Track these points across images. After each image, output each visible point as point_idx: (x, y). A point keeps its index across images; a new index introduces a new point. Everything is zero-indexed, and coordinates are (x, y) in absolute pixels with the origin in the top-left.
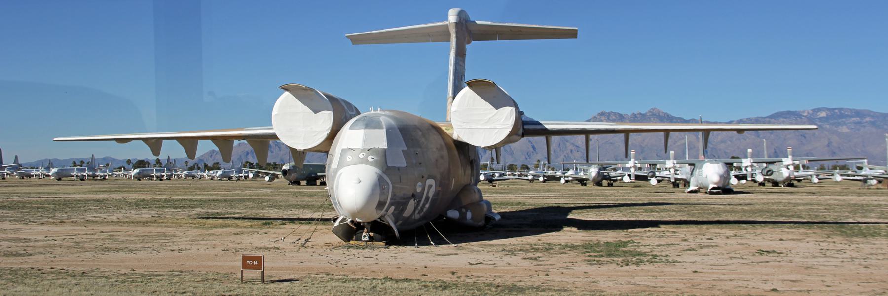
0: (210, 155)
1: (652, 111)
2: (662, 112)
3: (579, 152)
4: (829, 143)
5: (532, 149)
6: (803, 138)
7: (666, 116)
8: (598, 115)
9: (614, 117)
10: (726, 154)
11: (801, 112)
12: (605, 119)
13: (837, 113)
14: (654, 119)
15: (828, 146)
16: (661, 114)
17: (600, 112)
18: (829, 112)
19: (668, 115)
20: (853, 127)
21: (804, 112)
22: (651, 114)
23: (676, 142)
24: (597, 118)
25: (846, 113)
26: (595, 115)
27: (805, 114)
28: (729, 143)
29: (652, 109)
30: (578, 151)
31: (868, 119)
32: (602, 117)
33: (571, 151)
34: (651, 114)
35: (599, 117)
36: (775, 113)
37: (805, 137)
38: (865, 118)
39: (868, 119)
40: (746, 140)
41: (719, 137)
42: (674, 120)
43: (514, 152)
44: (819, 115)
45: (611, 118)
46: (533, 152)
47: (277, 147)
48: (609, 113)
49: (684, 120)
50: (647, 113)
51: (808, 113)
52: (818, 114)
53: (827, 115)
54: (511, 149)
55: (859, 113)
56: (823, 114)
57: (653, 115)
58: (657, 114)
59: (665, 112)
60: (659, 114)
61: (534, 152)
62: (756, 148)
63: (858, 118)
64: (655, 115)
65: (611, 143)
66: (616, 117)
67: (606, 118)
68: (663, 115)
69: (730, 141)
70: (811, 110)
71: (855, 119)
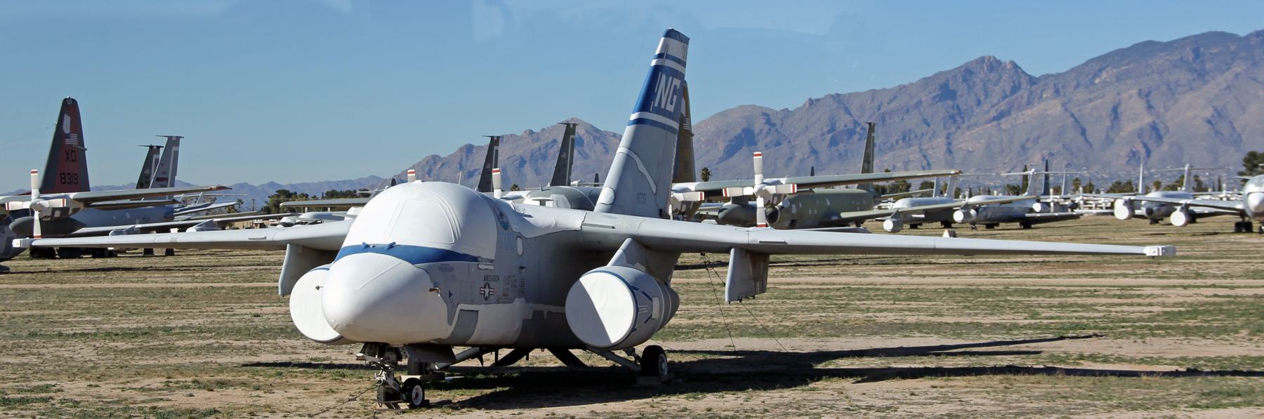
0: (427, 169)
43: (1244, 137)
47: (598, 144)
54: (1233, 128)
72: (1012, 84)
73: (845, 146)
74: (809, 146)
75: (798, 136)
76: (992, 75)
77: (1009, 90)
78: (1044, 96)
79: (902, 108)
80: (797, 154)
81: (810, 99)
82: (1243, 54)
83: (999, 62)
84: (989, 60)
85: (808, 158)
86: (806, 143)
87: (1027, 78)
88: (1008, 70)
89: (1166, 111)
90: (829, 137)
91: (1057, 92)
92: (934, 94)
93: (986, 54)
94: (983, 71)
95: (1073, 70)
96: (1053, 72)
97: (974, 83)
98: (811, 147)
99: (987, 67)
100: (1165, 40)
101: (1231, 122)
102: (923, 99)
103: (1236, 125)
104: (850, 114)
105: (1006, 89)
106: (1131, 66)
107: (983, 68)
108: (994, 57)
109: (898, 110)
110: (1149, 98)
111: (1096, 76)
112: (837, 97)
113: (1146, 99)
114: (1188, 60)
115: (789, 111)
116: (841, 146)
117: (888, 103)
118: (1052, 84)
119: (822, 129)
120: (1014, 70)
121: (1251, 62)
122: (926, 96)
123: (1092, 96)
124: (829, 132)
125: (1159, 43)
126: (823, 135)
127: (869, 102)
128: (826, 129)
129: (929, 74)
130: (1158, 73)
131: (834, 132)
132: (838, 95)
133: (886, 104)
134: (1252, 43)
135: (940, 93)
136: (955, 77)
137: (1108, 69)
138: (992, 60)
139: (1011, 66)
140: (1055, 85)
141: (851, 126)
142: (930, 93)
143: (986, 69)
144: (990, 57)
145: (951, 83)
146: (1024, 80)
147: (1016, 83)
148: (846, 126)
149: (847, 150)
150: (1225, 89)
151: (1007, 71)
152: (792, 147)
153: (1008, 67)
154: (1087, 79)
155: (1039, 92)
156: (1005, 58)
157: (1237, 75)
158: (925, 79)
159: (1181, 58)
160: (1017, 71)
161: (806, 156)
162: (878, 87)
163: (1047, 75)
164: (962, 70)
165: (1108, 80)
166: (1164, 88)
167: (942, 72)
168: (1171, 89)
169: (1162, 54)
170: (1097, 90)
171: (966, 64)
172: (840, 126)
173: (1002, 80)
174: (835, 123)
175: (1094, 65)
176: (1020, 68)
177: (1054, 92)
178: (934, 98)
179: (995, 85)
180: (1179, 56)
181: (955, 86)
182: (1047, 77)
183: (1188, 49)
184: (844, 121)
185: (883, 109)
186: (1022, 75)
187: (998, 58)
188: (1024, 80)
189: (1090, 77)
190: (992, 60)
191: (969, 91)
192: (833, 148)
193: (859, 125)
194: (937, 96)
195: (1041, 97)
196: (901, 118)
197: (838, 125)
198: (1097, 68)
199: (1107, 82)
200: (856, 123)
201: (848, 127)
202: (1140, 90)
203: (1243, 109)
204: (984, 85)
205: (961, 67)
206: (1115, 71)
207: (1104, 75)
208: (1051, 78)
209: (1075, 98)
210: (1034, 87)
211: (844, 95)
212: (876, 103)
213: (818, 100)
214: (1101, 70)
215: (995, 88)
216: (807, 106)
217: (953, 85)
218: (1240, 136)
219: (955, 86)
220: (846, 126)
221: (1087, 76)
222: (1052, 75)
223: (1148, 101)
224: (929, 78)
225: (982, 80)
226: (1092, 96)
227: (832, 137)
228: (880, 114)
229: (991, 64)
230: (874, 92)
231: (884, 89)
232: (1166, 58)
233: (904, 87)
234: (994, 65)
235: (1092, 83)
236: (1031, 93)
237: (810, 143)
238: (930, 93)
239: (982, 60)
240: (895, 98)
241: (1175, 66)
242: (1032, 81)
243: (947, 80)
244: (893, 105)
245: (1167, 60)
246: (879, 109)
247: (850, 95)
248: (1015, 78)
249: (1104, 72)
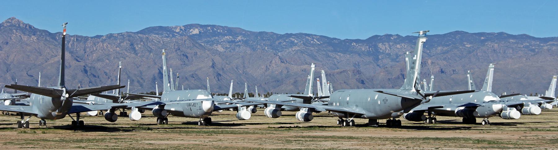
1: (10, 21)
2: (24, 24)
4: (213, 64)
6: (185, 58)
7: (28, 27)
10: (106, 75)
11: (173, 28)
13: (209, 30)
14: (17, 32)
15: (213, 66)
16: (21, 25)
18: (201, 29)
19: (30, 27)
20: (228, 46)
21: (176, 28)
22: (8, 24)
23: (48, 59)
25: (219, 31)
27: (178, 31)
28: (107, 61)
29: (10, 18)
31: (239, 38)
34: (8, 24)
36: (146, 29)
37: (187, 57)
38: (238, 37)
39: (239, 38)
40: (125, 59)
41: (94, 55)
42: (38, 33)
44: (192, 32)
49: (50, 34)
50: (3, 23)
51: (181, 30)
52: (190, 31)
53: (200, 32)
55: (230, 31)
56: (196, 31)
57: (12, 25)
58: (17, 25)
59: (26, 23)
60: (19, 25)
62: (138, 68)
63: (231, 37)
64: (15, 26)
68: (24, 26)
69: (108, 59)
70: (183, 26)
71: (228, 37)
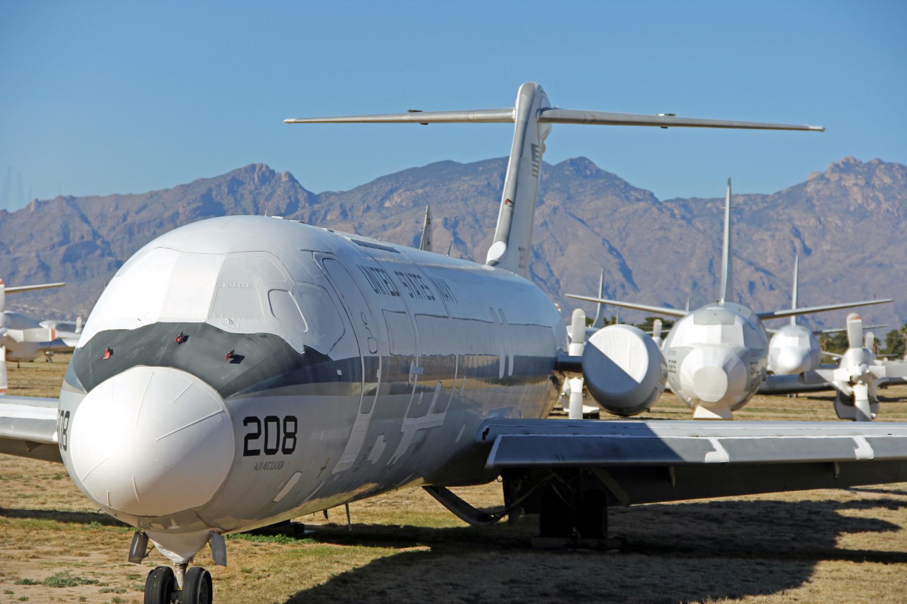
3: (777, 292)
5: (619, 277)
8: (833, 171)
9: (887, 180)
12: (856, 184)
17: (839, 159)
24: (828, 180)
26: (822, 170)
30: (772, 288)
32: (844, 176)
33: (752, 285)
35: (834, 177)
43: (561, 283)
45: (876, 182)
46: (623, 286)
48: (869, 164)
54: (551, 271)
61: (627, 284)
65: (880, 265)
66: (894, 178)
67: (862, 182)
72: (288, 201)
73: (83, 262)
74: (36, 260)
75: (20, 245)
76: (263, 188)
77: (284, 207)
78: (328, 218)
79: (155, 220)
80: (20, 269)
81: (37, 201)
82: (558, 185)
83: (272, 172)
84: (260, 169)
85: (35, 274)
86: (33, 255)
87: (305, 194)
88: (284, 182)
89: (474, 246)
90: (62, 250)
91: (344, 214)
92: (194, 206)
93: (257, 161)
94: (254, 182)
95: (359, 189)
96: (336, 190)
97: (242, 196)
98: (40, 261)
99: (259, 177)
100: (465, 161)
101: (548, 265)
102: (180, 211)
103: (554, 269)
104: (84, 219)
105: (280, 206)
106: (427, 189)
107: (254, 179)
108: (267, 167)
109: (149, 222)
110: (457, 230)
111: (388, 196)
112: (71, 200)
113: (452, 230)
114: (496, 187)
115: (7, 213)
116: (79, 264)
117: (137, 213)
118: (338, 203)
119: (52, 239)
120: (291, 183)
121: (566, 195)
122: (184, 207)
123: (387, 221)
124: (61, 244)
125: (460, 165)
126: (53, 247)
127: (111, 210)
128: (57, 240)
129: (188, 181)
130: (462, 200)
131: (70, 244)
132: (73, 199)
133: (133, 214)
134: (567, 173)
135: (201, 204)
136: (219, 186)
137: (401, 191)
138: (264, 169)
139: (287, 179)
140: (341, 205)
141: (88, 238)
142: (189, 204)
143: (256, 179)
144: (262, 165)
145: (214, 193)
146: (301, 197)
147: (293, 199)
148: (82, 237)
149: (85, 268)
150: (542, 225)
151: (282, 184)
152: (15, 259)
153: (284, 179)
154: (375, 201)
155: (323, 212)
156: (280, 169)
157: (555, 210)
158: (183, 186)
159: (489, 184)
160: (294, 186)
161: (33, 272)
162: (123, 192)
163: (328, 192)
164: (229, 178)
165: (404, 204)
166: (470, 219)
167: (204, 180)
168: (477, 221)
169: (466, 178)
170: (391, 215)
171: (233, 172)
172: (75, 238)
173: (276, 195)
174: (69, 233)
175: (384, 184)
176: (297, 182)
177: (341, 214)
178: (195, 210)
179: (267, 200)
180: (486, 182)
181: (219, 197)
182: (328, 194)
183: (496, 174)
184: (80, 232)
185: (129, 220)
186: (299, 190)
187: (271, 168)
188: (301, 197)
189: (379, 198)
190: (264, 169)
191: (236, 206)
192: (68, 265)
193: (100, 237)
194: (198, 208)
195: (325, 219)
196: (152, 231)
197: (72, 235)
198: (387, 189)
199: (402, 206)
200: (95, 234)
201: (85, 239)
202: (446, 219)
203: (561, 250)
204: (254, 198)
205: (227, 175)
206: (408, 193)
207: (396, 198)
208: (333, 197)
209: (366, 223)
210: (316, 207)
211: (81, 198)
212: (120, 212)
213: (46, 203)
214: (392, 192)
215: (266, 203)
216: (32, 208)
217: (216, 196)
218: (558, 281)
219: (219, 197)
220: (82, 237)
221: (375, 197)
222: (334, 193)
223: (455, 234)
224: (188, 186)
225: (251, 192)
226: (387, 221)
227: (68, 249)
228: (126, 225)
229: (263, 174)
230: (117, 198)
231: (131, 196)
232: (472, 182)
233: (157, 193)
234: (268, 176)
235: (381, 206)
236: (314, 213)
237: (38, 256)
238: (189, 204)
239: (253, 167)
240: (145, 206)
241: (481, 193)
242: (312, 198)
243: (210, 190)
244: (143, 215)
245: (473, 186)
246: (125, 218)
247: (87, 199)
248: (291, 194)
249: (395, 195)
